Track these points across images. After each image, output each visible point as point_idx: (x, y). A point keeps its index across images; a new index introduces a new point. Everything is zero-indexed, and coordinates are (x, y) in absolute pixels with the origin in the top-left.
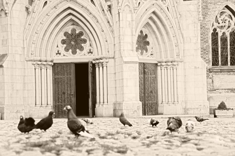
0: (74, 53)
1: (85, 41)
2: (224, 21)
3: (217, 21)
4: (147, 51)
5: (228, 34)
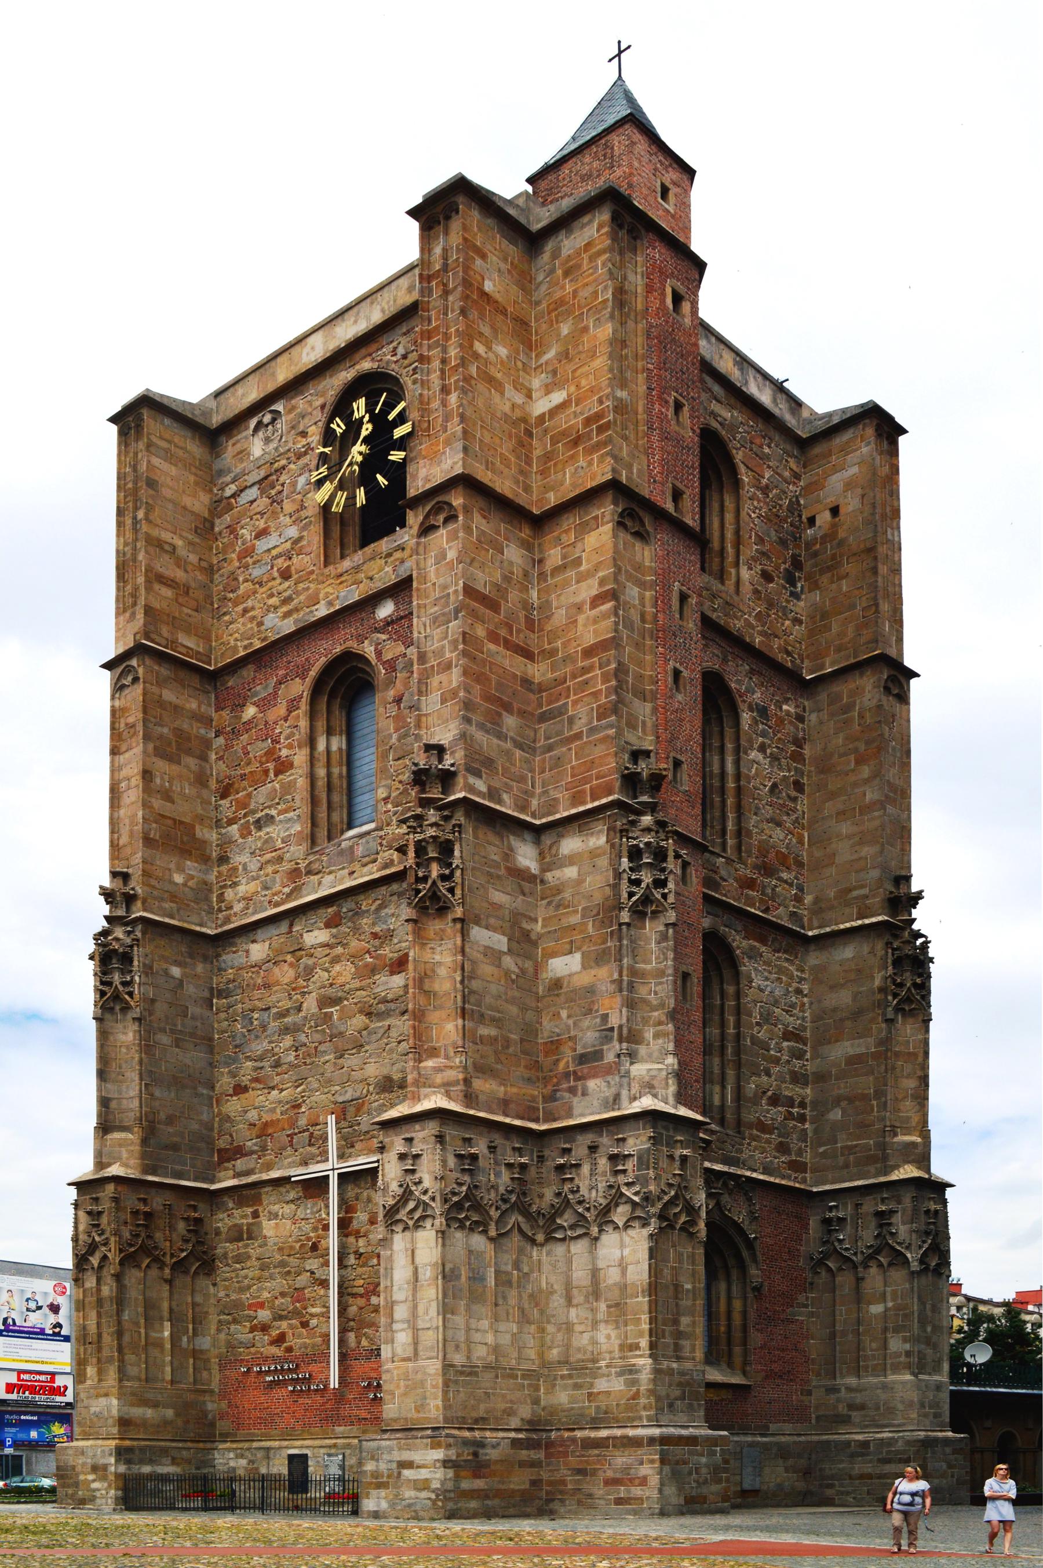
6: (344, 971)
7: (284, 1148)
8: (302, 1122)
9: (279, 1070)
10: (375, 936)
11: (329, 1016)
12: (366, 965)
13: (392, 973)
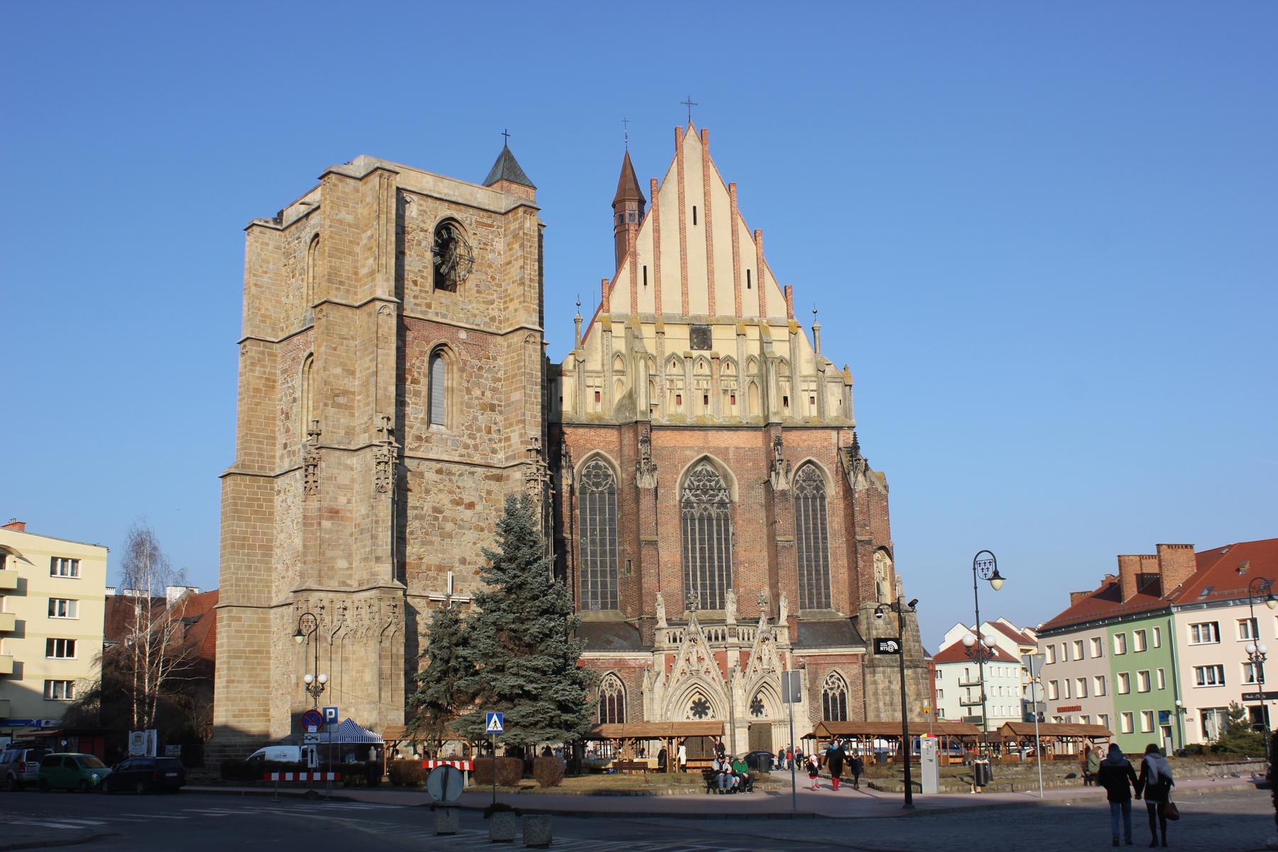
0: (700, 717)
1: (708, 708)
2: (833, 683)
3: (827, 683)
4: (761, 713)
5: (837, 694)
6: (445, 499)
7: (414, 578)
8: (424, 567)
9: (413, 537)
10: (459, 488)
11: (436, 519)
12: (455, 500)
13: (466, 508)
